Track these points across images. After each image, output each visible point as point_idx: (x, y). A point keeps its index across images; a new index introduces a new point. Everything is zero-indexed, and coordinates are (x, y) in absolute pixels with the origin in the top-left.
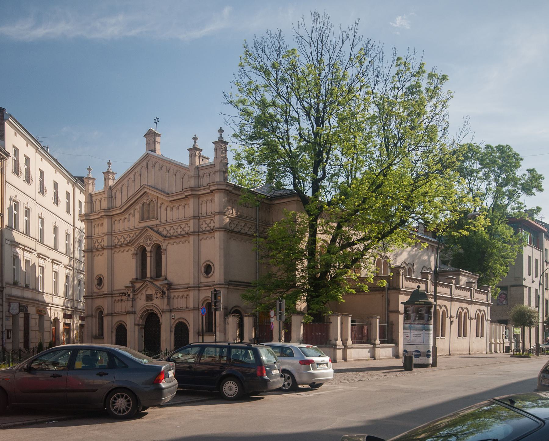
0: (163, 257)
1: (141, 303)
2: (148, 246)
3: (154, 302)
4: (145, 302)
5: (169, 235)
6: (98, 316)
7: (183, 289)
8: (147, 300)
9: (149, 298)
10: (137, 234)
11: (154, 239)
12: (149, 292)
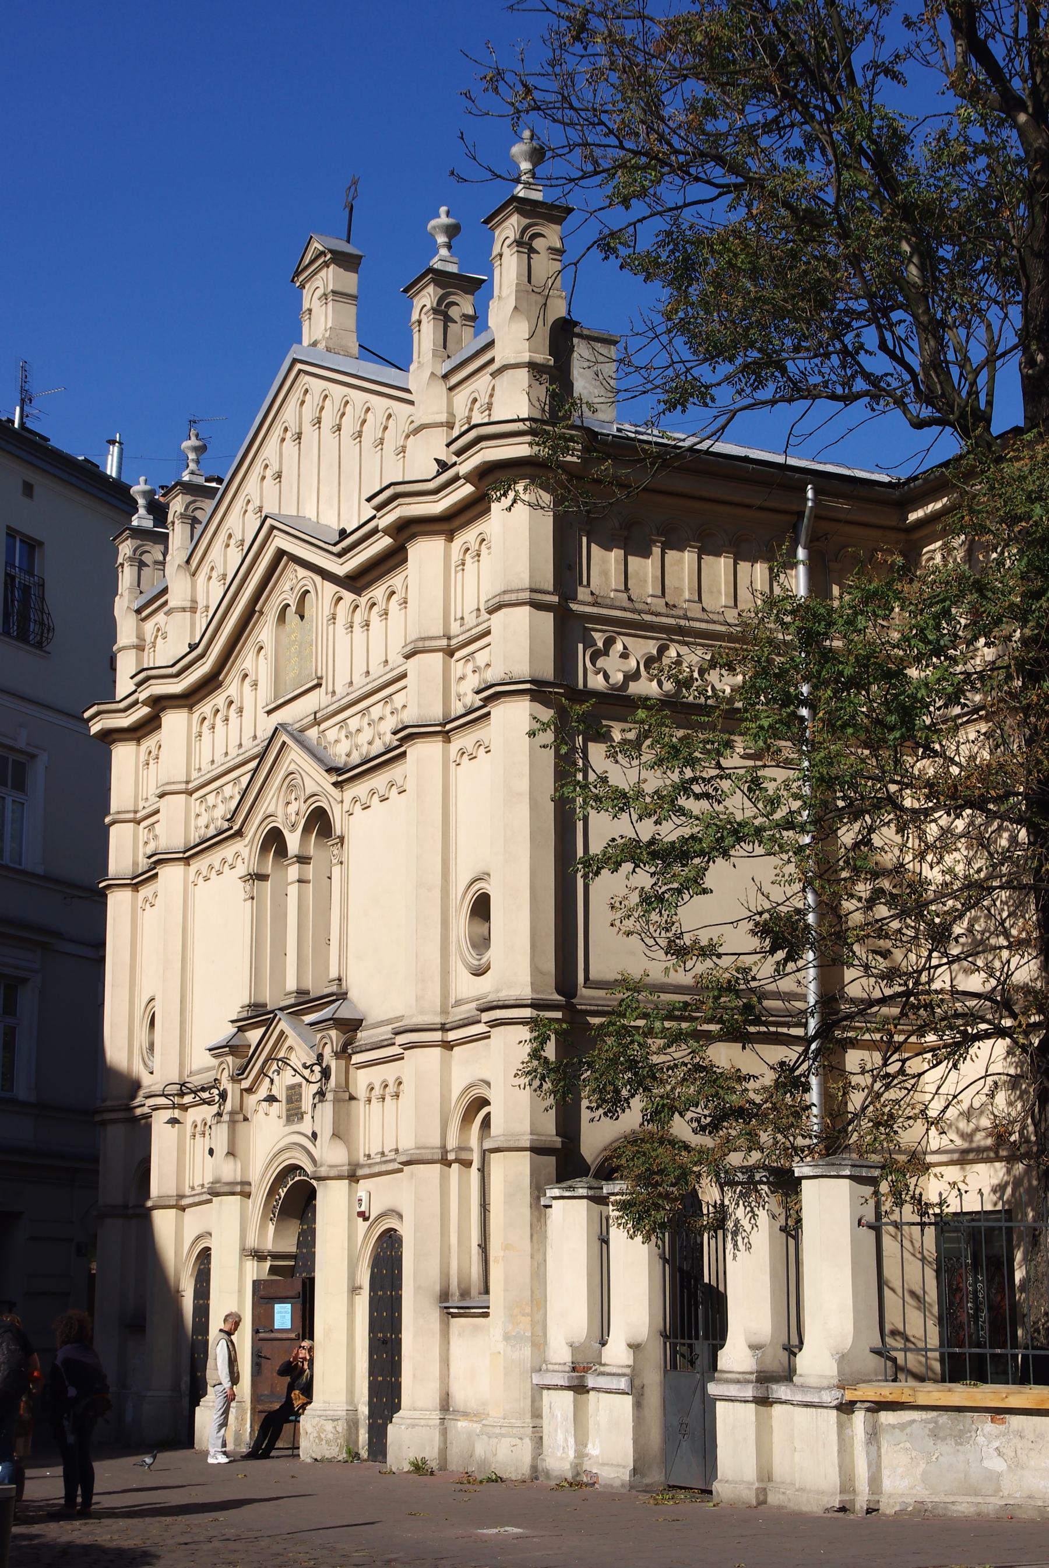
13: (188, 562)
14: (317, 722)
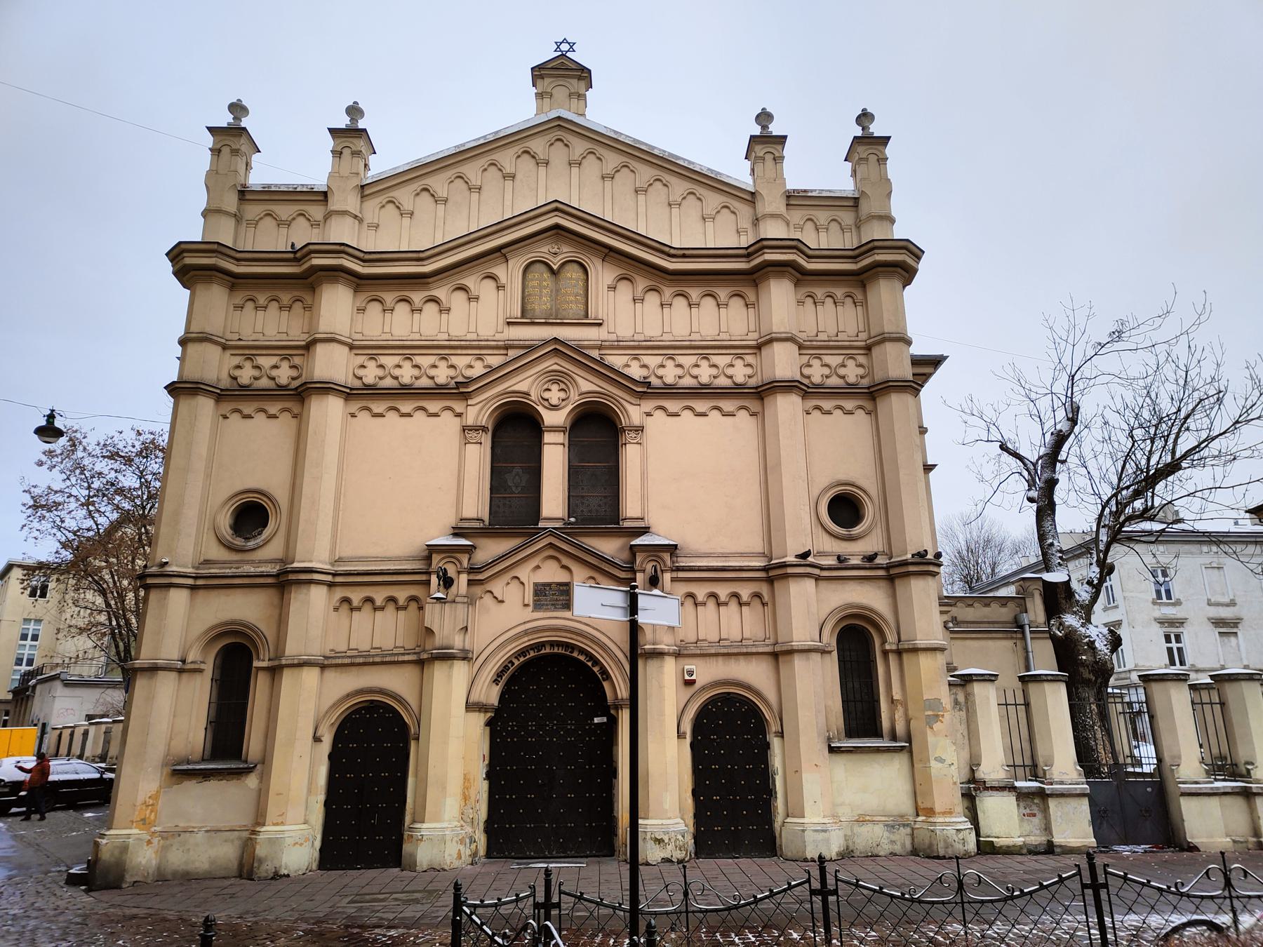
0: (631, 456)
1: (502, 619)
2: (554, 408)
4: (528, 614)
5: (655, 382)
6: (209, 668)
7: (741, 569)
10: (495, 361)
11: (585, 386)
12: (551, 573)
14: (600, 348)
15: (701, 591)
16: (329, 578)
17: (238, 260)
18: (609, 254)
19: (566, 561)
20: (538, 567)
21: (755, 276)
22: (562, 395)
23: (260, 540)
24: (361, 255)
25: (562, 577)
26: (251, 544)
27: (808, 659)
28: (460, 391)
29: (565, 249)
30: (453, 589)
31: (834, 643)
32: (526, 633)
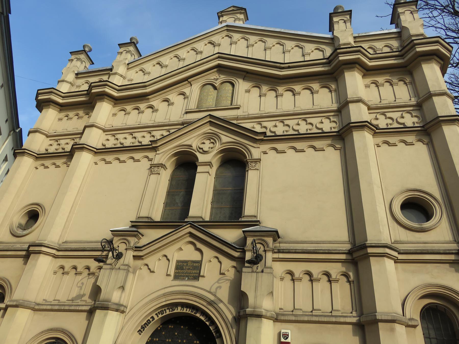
2: (205, 152)
3: (201, 283)
4: (170, 281)
8: (176, 277)
9: (188, 271)
12: (189, 253)
13: (128, 64)
15: (298, 269)
16: (54, 252)
17: (63, 97)
18: (247, 75)
19: (199, 245)
20: (181, 249)
21: (335, 74)
22: (212, 145)
23: (30, 230)
24: (117, 87)
25: (196, 256)
26: (25, 232)
27: (392, 330)
28: (153, 147)
29: (222, 76)
30: (121, 261)
31: (418, 318)
32: (164, 295)
